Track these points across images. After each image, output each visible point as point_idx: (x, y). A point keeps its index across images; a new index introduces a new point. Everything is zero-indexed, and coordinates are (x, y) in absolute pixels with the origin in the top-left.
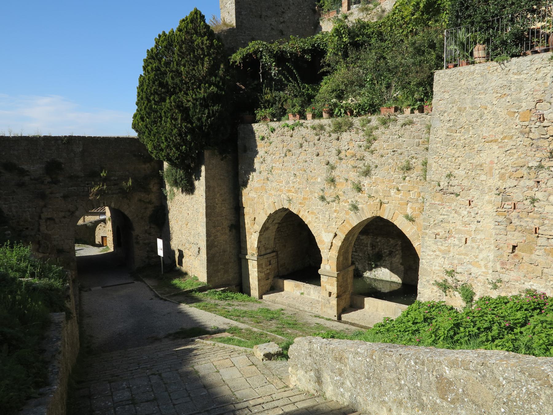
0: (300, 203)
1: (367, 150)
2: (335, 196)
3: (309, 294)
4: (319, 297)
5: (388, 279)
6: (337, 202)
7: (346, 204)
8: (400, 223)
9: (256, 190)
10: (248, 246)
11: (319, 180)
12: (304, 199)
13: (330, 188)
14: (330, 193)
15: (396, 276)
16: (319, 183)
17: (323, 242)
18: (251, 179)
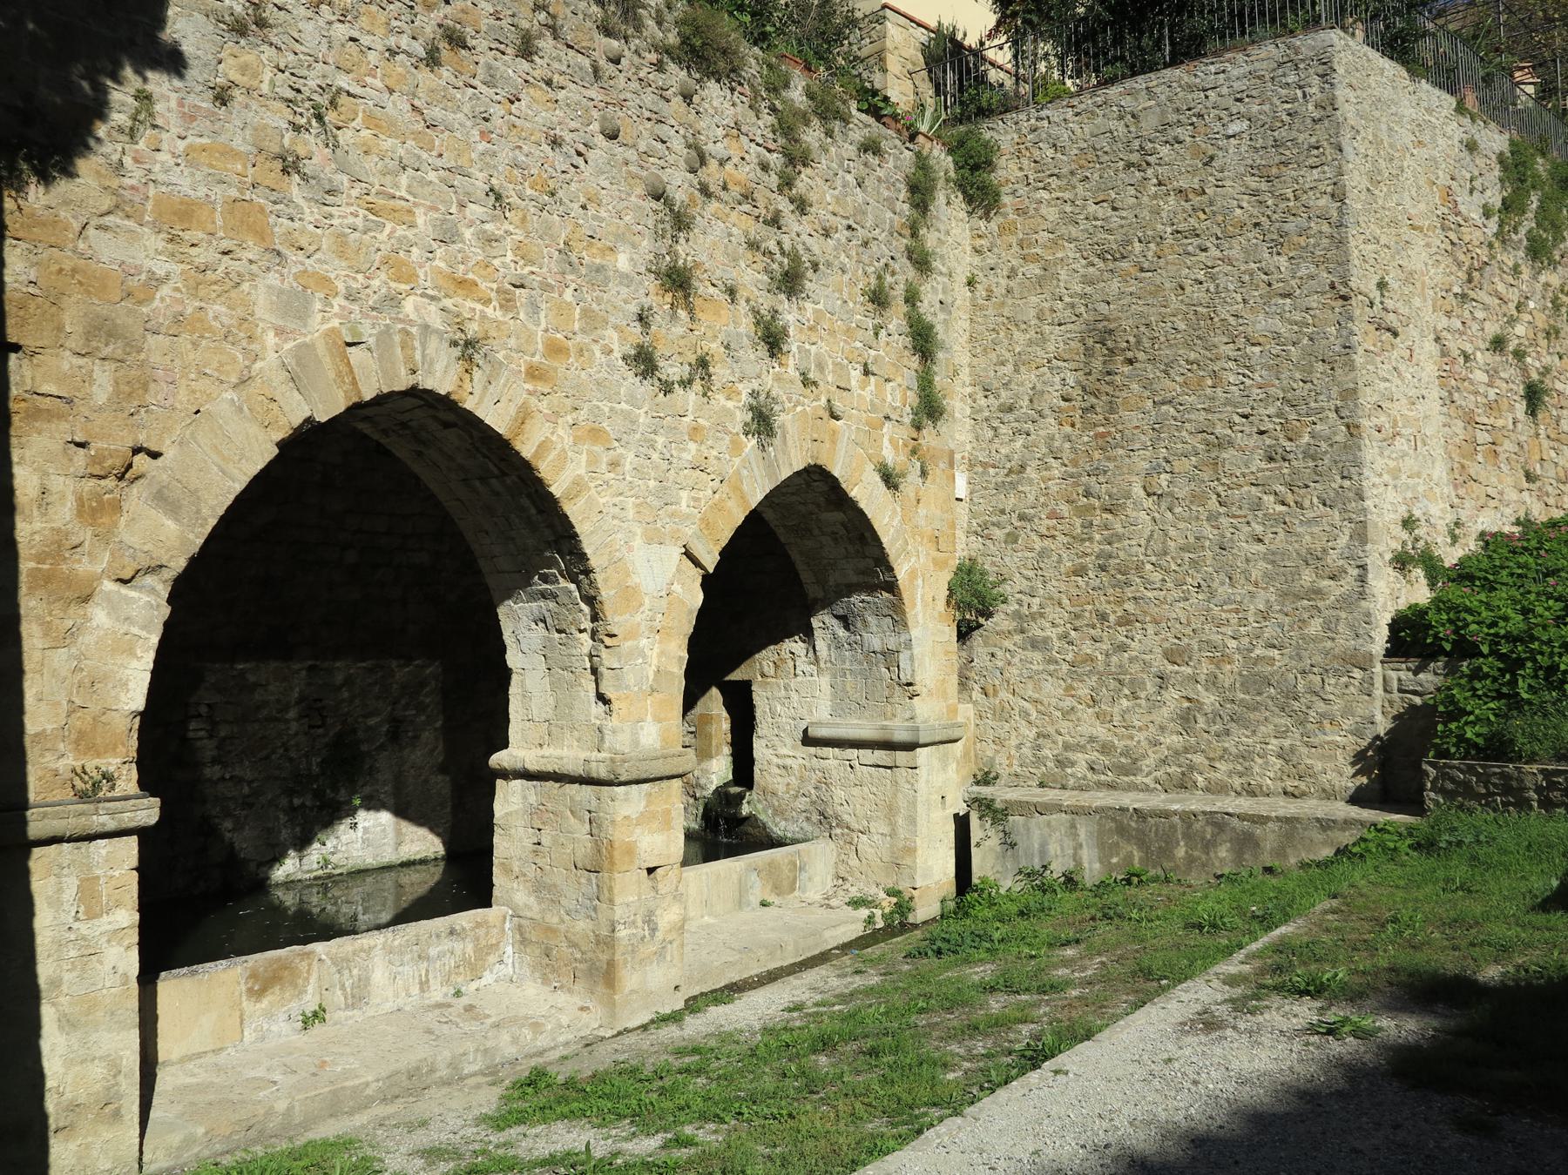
0: (534, 373)
1: (786, 191)
2: (693, 359)
3: (358, 996)
4: (424, 985)
5: (389, 856)
6: (697, 386)
7: (730, 404)
8: (866, 492)
9: (178, 218)
10: (39, 716)
11: (623, 262)
12: (555, 350)
13: (674, 317)
14: (674, 341)
15: (423, 832)
16: (625, 279)
17: (630, 595)
18: (119, 118)
